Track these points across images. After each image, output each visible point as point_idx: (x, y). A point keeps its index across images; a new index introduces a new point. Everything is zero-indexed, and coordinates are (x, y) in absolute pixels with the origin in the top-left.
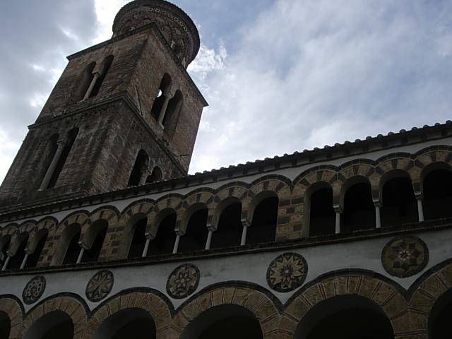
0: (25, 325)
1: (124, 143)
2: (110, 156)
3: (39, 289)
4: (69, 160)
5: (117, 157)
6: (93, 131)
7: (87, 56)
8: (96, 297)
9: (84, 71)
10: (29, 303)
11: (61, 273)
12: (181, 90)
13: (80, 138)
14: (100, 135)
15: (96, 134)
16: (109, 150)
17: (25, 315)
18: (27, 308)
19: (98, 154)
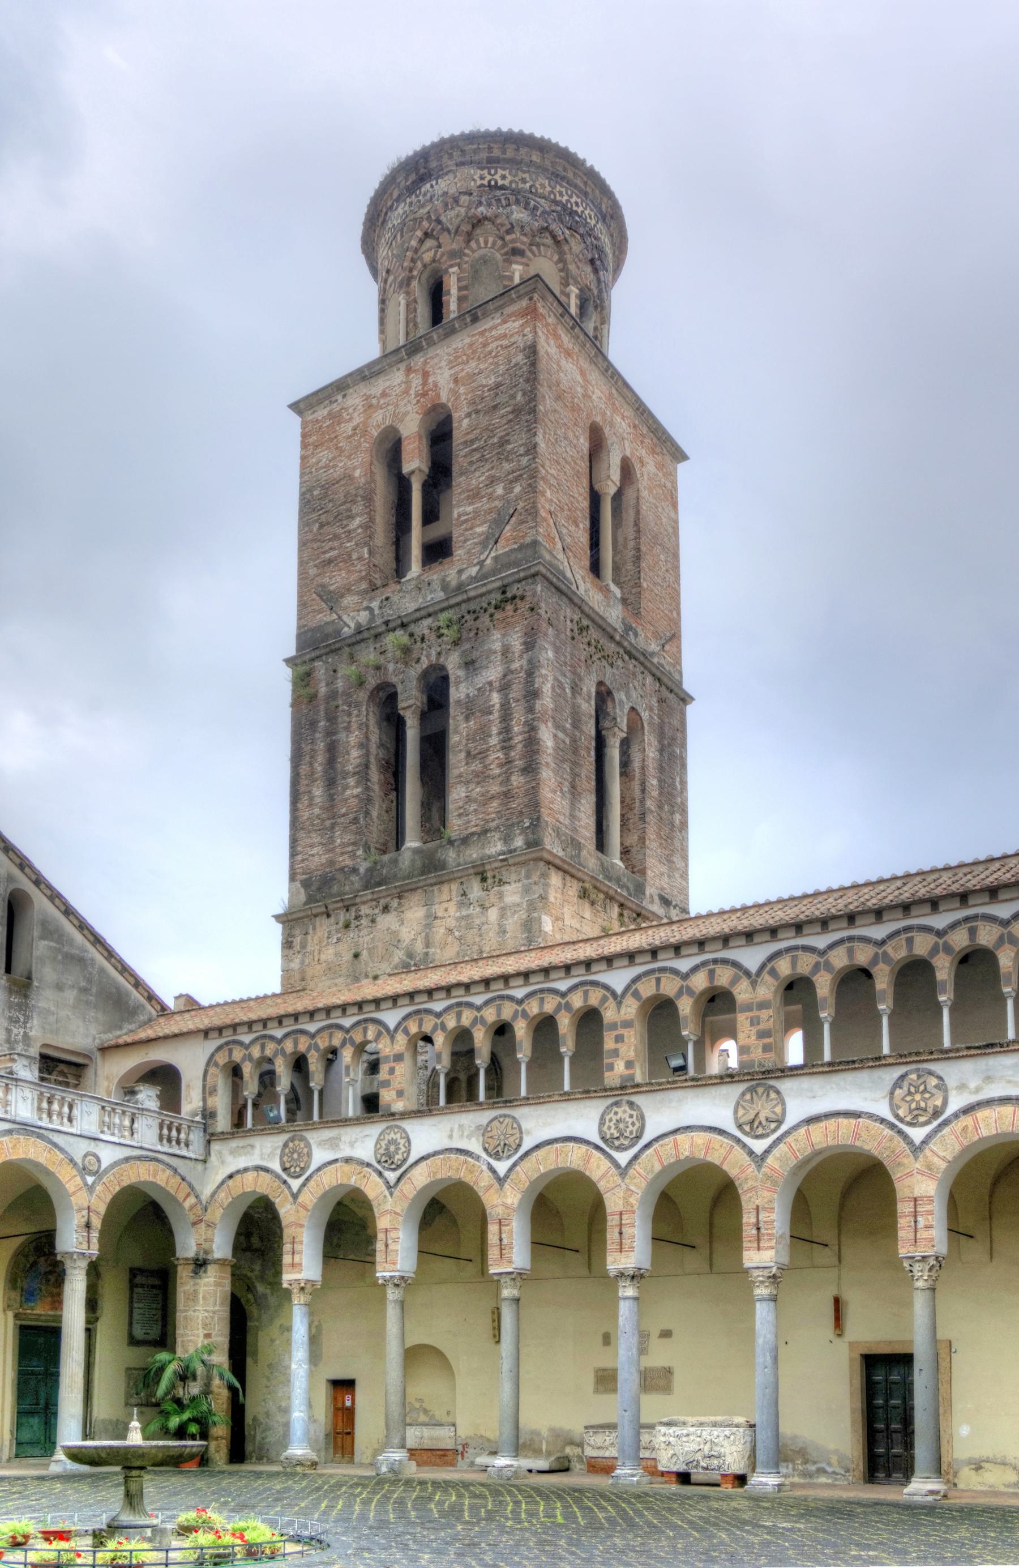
1: (568, 690)
2: (555, 736)
4: (457, 763)
5: (564, 730)
6: (493, 673)
7: (354, 400)
8: (760, 1131)
9: (371, 464)
10: (621, 1148)
11: (667, 1093)
12: (628, 453)
13: (463, 696)
14: (517, 691)
15: (505, 688)
16: (550, 724)
17: (623, 1172)
19: (532, 743)
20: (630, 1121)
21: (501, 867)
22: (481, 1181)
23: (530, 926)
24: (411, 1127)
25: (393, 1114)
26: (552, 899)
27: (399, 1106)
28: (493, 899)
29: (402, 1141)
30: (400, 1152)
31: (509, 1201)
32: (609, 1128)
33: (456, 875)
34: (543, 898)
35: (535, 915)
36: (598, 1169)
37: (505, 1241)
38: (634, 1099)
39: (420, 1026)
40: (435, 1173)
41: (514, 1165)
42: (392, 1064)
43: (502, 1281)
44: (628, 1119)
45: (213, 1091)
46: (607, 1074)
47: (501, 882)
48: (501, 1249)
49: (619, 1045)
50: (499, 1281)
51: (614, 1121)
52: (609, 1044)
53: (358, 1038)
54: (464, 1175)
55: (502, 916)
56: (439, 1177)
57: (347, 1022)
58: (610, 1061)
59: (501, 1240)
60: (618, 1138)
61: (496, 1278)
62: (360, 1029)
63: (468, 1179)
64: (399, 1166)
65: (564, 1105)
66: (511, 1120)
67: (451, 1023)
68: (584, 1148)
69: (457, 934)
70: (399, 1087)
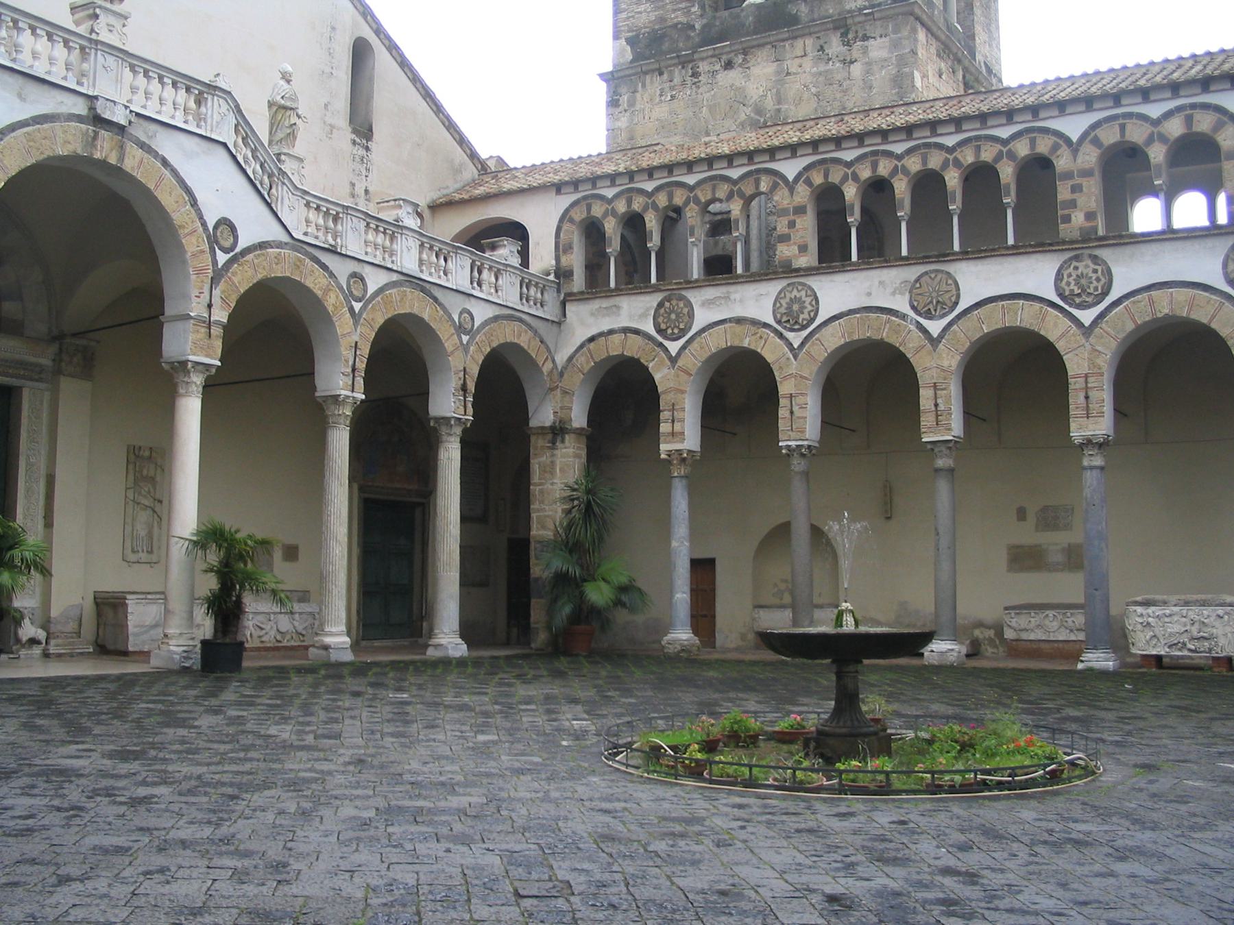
0: (1099, 348)
3: (1098, 280)
10: (1083, 306)
18: (1087, 316)
20: (1094, 276)
21: (865, 21)
22: (910, 344)
23: (901, 81)
24: (816, 283)
25: (797, 270)
26: (920, 55)
27: (803, 262)
28: (856, 53)
29: (808, 300)
30: (806, 311)
31: (946, 363)
32: (1068, 284)
33: (812, 30)
34: (914, 52)
35: (907, 70)
36: (1054, 329)
37: (941, 407)
38: (1097, 252)
39: (826, 176)
40: (850, 334)
41: (950, 324)
42: (792, 217)
43: (936, 450)
44: (1091, 274)
45: (568, 248)
46: (1062, 227)
47: (865, 38)
48: (937, 416)
49: (1075, 196)
50: (932, 450)
51: (1074, 276)
52: (1064, 193)
53: (749, 190)
54: (886, 335)
55: (868, 72)
56: (856, 337)
57: (735, 173)
58: (1066, 212)
59: (936, 405)
60: (1079, 295)
61: (929, 447)
62: (751, 180)
63: (894, 340)
64: (804, 327)
65: (1010, 259)
66: (944, 276)
67: (865, 173)
68: (1037, 305)
69: (814, 90)
70: (801, 241)
